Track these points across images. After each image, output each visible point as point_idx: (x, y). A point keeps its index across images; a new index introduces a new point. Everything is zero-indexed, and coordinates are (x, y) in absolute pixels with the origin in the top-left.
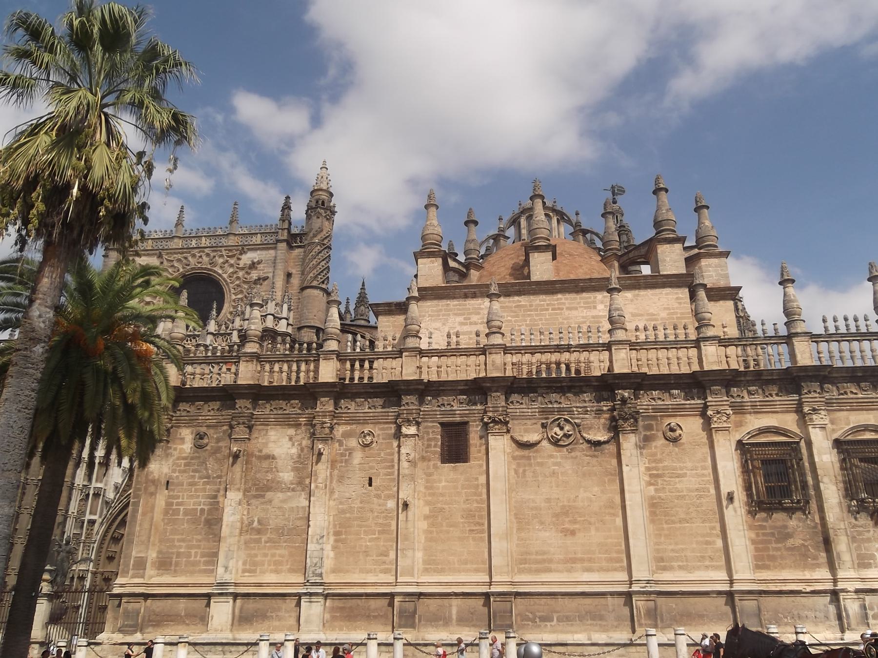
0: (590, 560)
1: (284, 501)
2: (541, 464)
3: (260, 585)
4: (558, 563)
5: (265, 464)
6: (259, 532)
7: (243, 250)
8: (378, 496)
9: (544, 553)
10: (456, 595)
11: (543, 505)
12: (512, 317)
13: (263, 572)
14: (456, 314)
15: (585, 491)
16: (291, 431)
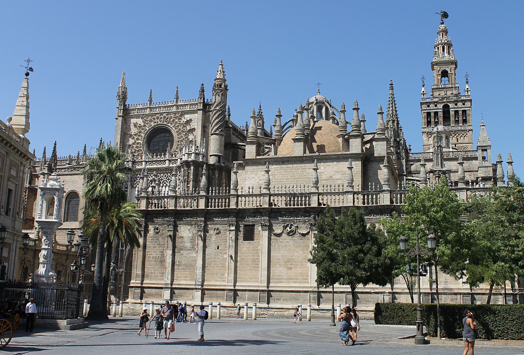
0: (296, 279)
1: (187, 254)
2: (281, 242)
3: (180, 285)
4: (285, 280)
5: (180, 240)
6: (179, 265)
7: (183, 113)
8: (221, 253)
9: (280, 276)
10: (248, 290)
11: (281, 258)
12: (284, 172)
13: (181, 280)
14: (261, 171)
15: (297, 253)
16: (189, 227)
